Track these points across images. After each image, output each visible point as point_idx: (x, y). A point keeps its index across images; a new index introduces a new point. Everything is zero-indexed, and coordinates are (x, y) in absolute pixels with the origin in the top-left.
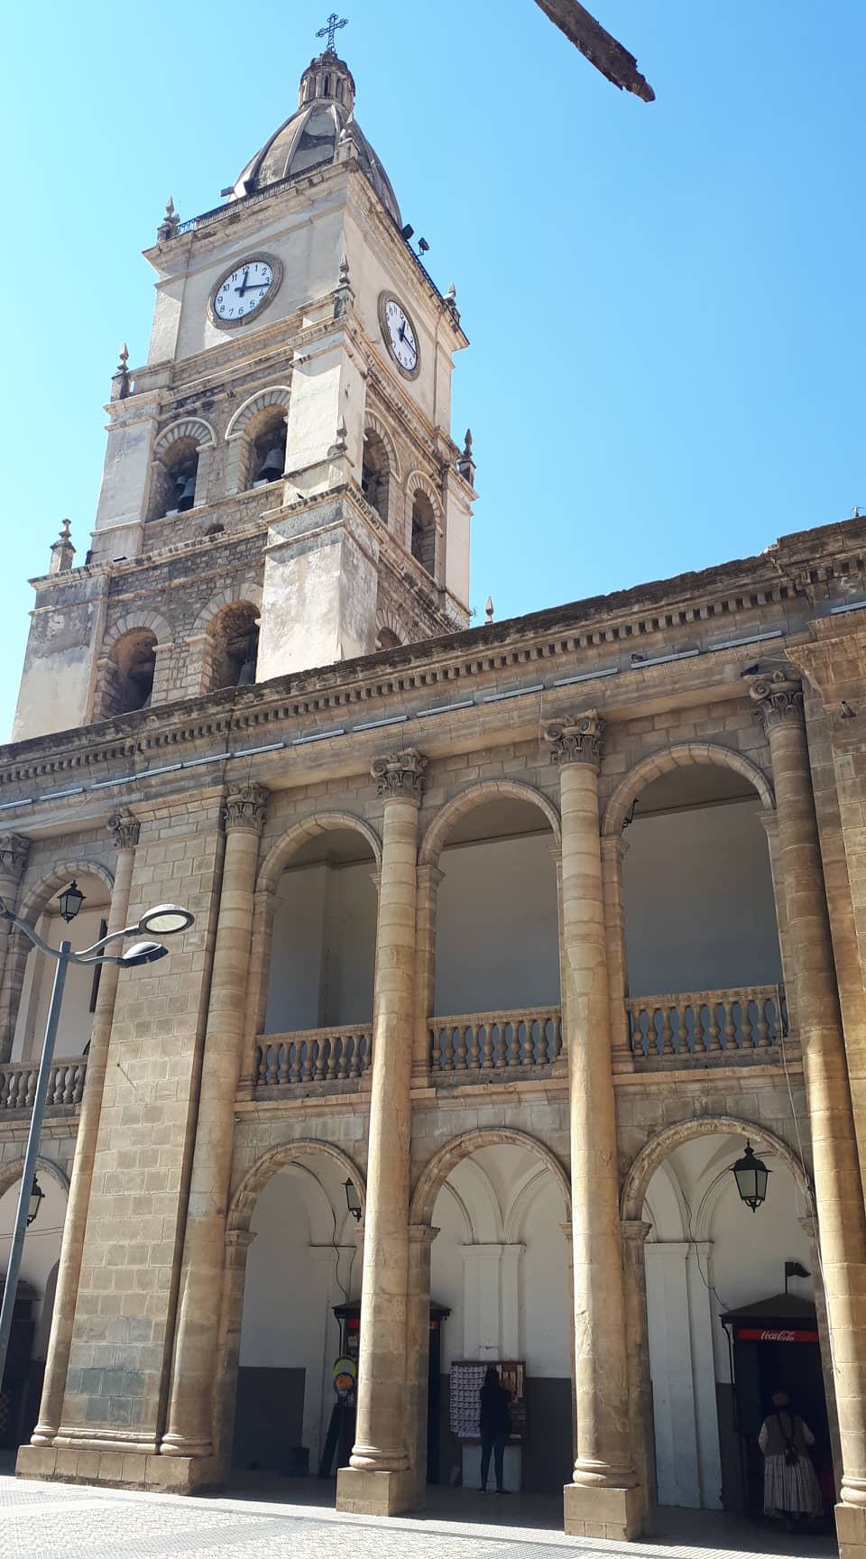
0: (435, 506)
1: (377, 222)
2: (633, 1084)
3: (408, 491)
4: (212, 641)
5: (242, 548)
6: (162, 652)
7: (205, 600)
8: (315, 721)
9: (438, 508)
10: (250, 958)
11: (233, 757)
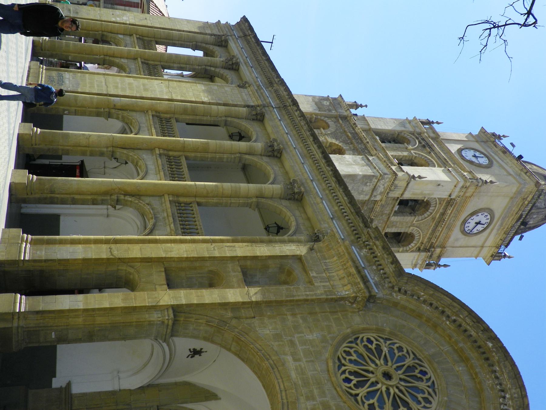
0: (410, 246)
1: (521, 204)
2: (165, 199)
3: (411, 228)
4: (328, 145)
5: (366, 151)
6: (321, 131)
7: (344, 142)
8: (290, 127)
9: (410, 249)
10: (202, 116)
11: (274, 108)
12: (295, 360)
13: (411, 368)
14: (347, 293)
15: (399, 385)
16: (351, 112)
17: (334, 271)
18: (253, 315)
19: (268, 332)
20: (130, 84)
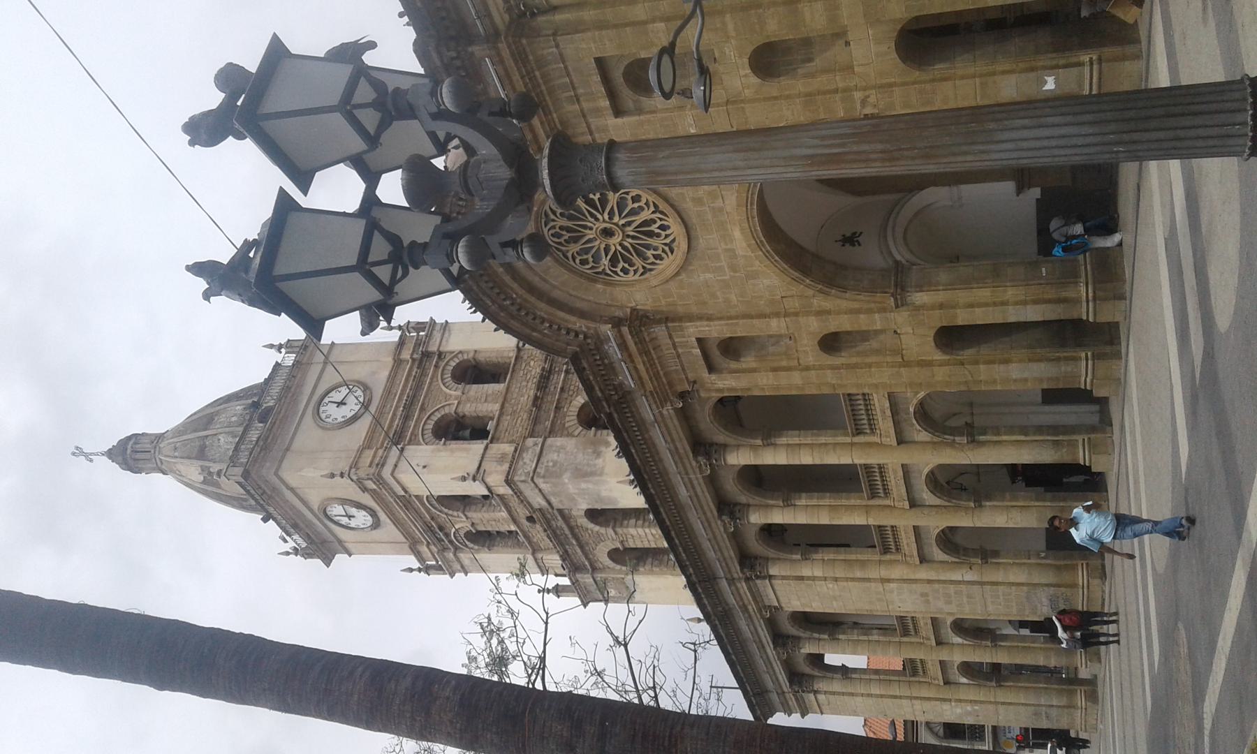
0: (458, 361)
1: (269, 441)
3: (459, 393)
4: (611, 524)
12: (733, 250)
13: (575, 240)
16: (570, 579)
18: (784, 299)
20: (949, 603)
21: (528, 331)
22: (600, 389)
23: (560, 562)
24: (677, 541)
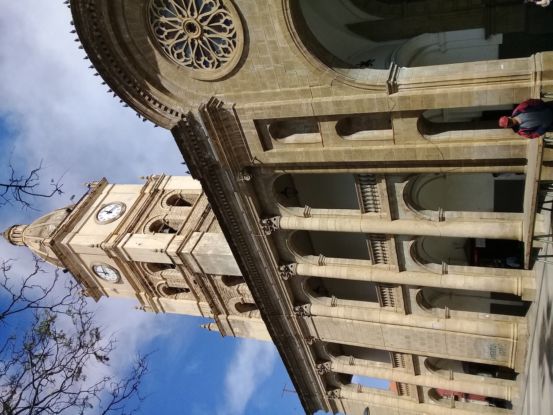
0: (171, 194)
3: (168, 209)
12: (274, 42)
14: (225, 111)
15: (183, 18)
17: (235, 135)
19: (298, 71)
20: (423, 344)
21: (144, 108)
22: (195, 159)
23: (210, 309)
24: (253, 283)
